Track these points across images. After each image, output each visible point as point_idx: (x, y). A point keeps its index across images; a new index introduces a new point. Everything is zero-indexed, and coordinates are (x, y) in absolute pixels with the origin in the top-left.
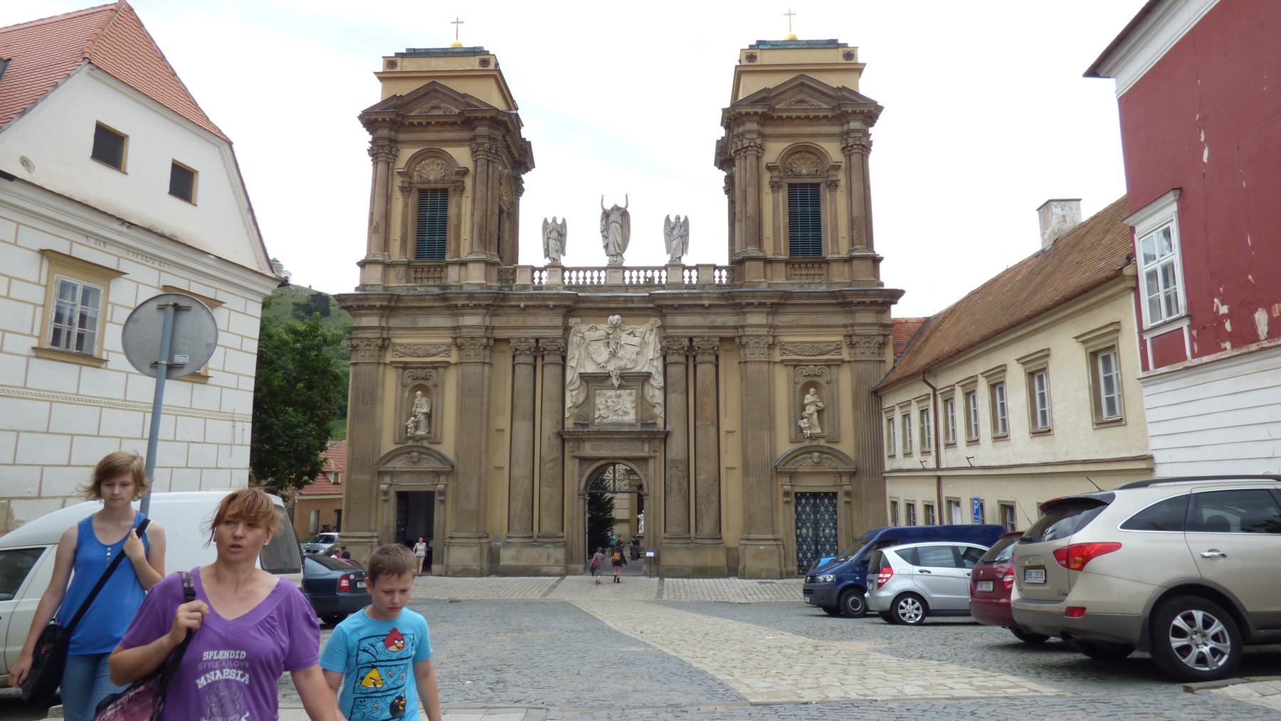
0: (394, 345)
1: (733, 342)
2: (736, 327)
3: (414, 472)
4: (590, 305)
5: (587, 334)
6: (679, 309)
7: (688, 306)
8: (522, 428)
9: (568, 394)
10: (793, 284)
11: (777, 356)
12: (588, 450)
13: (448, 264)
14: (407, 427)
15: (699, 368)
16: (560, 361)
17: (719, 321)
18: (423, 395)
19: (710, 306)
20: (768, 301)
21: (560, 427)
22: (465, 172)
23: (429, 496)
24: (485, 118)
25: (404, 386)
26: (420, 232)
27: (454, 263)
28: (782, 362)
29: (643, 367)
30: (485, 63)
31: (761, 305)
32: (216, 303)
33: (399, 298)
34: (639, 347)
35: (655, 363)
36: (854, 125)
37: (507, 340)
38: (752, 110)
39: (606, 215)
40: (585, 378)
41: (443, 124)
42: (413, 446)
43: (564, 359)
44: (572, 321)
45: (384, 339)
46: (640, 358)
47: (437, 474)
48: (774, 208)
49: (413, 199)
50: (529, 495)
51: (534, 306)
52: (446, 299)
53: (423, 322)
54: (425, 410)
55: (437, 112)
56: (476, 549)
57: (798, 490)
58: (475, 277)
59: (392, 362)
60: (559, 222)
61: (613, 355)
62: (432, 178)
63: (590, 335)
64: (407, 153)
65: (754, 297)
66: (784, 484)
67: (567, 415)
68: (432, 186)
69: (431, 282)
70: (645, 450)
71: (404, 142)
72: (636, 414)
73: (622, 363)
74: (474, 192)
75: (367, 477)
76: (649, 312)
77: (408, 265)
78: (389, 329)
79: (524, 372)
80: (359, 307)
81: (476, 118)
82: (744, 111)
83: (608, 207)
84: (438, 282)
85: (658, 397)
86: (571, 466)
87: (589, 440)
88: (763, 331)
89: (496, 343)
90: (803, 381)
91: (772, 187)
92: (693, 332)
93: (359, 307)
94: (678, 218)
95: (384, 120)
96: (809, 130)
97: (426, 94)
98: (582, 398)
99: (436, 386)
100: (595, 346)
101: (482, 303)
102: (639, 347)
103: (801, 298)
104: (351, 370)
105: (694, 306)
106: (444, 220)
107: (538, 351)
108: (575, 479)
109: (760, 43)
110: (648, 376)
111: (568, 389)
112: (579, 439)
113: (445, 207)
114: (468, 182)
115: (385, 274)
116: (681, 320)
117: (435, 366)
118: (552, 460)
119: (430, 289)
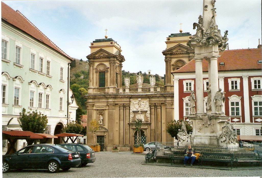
2: (164, 101)
3: (100, 132)
5: (134, 102)
8: (122, 123)
9: (130, 115)
13: (105, 88)
16: (129, 108)
17: (161, 100)
19: (159, 96)
21: (129, 122)
22: (108, 68)
23: (103, 136)
24: (112, 57)
25: (98, 114)
27: (106, 88)
29: (145, 110)
30: (112, 43)
33: (96, 96)
35: (148, 108)
36: (191, 55)
38: (168, 53)
40: (134, 112)
43: (130, 108)
44: (131, 100)
46: (145, 107)
47: (105, 132)
49: (98, 74)
50: (123, 136)
51: (123, 97)
52: (105, 96)
53: (101, 100)
54: (102, 119)
55: (102, 55)
58: (111, 91)
59: (95, 109)
61: (140, 107)
62: (102, 69)
63: (135, 103)
64: (96, 64)
65: (168, 95)
67: (130, 120)
70: (146, 127)
71: (95, 62)
72: (145, 120)
73: (141, 109)
76: (147, 98)
78: (94, 102)
79: (122, 110)
81: (110, 57)
84: (104, 92)
86: (131, 130)
88: (170, 102)
92: (156, 102)
96: (181, 56)
98: (133, 116)
99: (104, 114)
101: (113, 97)
102: (145, 105)
104: (87, 110)
105: (156, 96)
106: (105, 78)
107: (124, 106)
109: (172, 34)
110: (146, 111)
111: (131, 114)
113: (105, 76)
114: (109, 70)
116: (153, 99)
117: (103, 110)
118: (127, 129)
119: (102, 94)
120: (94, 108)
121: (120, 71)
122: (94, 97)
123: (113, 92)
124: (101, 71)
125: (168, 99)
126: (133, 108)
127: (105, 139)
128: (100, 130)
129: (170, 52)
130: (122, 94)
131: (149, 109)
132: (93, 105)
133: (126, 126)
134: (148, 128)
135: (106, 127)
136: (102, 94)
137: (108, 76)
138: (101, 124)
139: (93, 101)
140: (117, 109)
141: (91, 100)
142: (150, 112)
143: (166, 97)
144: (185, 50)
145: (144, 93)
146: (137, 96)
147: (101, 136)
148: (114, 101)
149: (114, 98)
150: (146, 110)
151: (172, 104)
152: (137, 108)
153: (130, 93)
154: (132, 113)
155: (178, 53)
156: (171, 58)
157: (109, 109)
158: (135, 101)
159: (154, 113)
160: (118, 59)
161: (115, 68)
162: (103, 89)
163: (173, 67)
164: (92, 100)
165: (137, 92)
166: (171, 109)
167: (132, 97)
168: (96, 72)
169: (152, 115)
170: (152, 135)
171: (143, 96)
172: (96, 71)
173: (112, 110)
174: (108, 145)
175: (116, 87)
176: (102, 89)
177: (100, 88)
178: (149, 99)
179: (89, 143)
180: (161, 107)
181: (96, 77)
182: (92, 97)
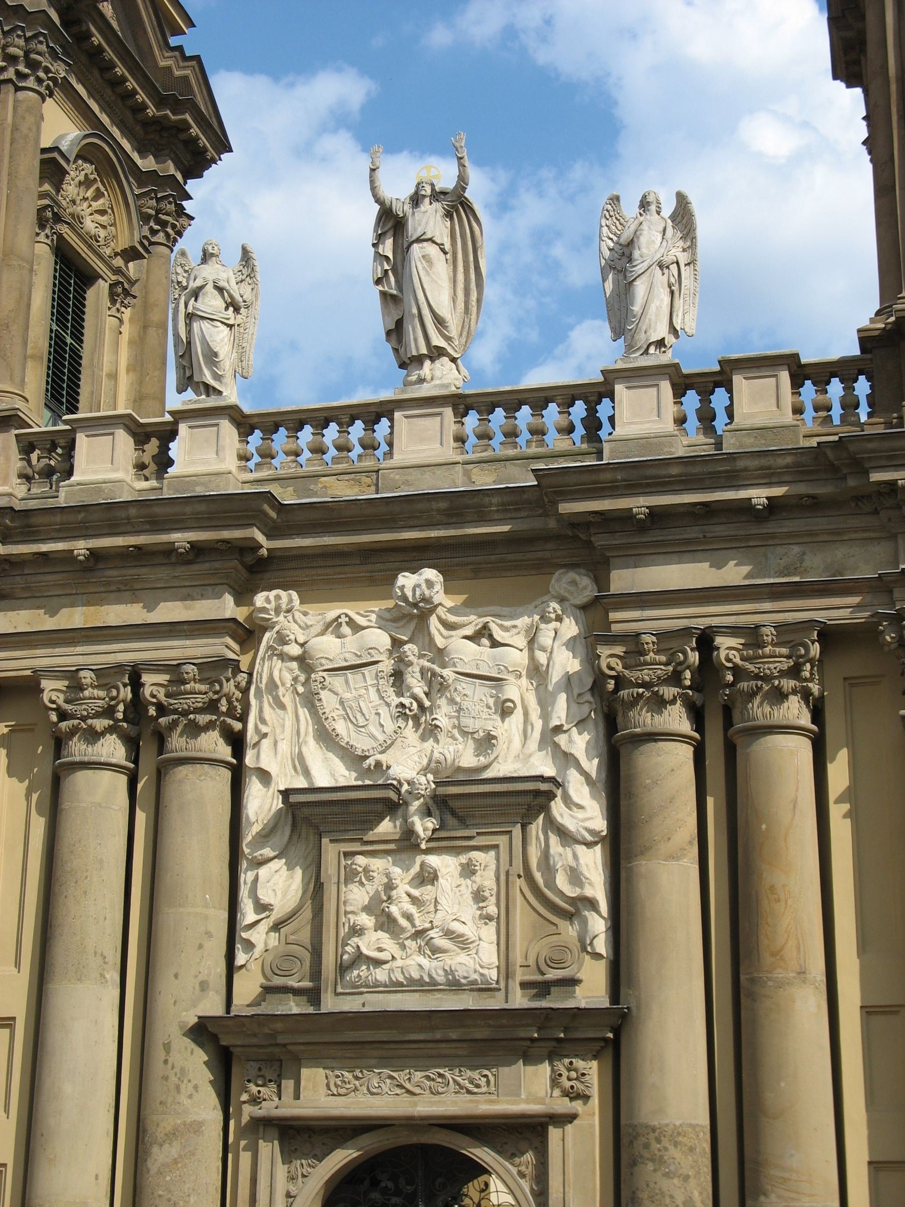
6: (661, 533)
9: (246, 877)
12: (318, 1092)
34: (509, 685)
43: (237, 742)
67: (241, 958)
70: (528, 1088)
126: (290, 755)
134: (571, 1118)
152: (361, 744)
167: (274, 557)
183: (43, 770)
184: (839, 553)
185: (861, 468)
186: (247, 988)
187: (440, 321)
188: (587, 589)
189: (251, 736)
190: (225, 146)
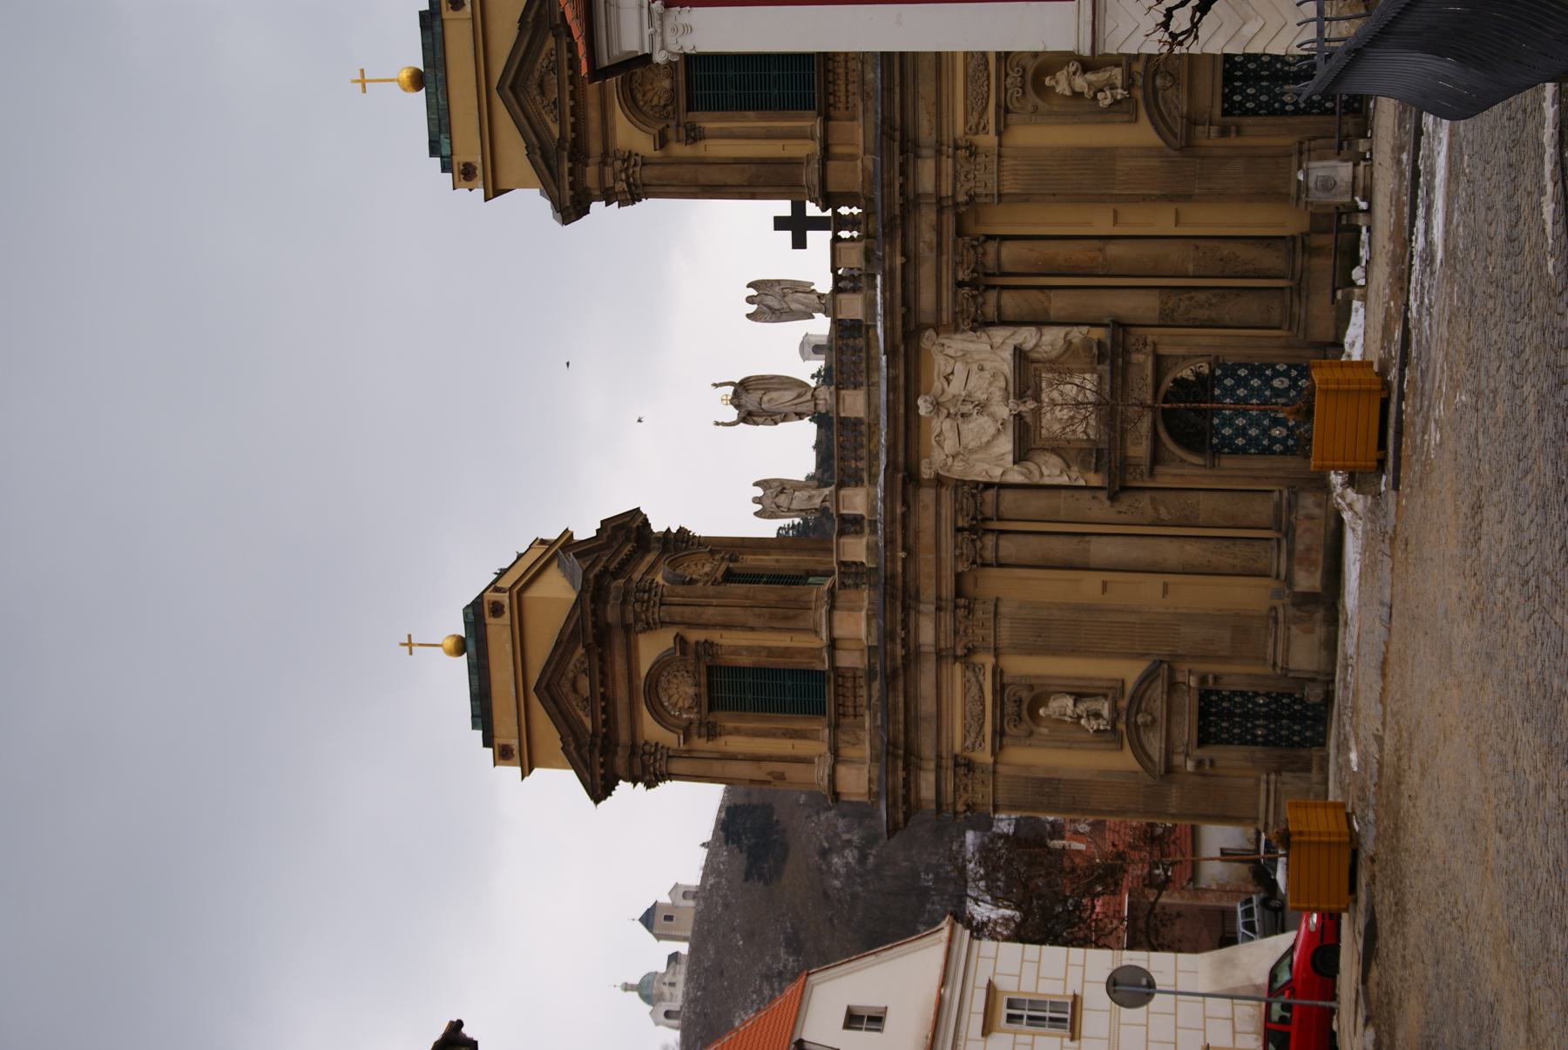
0: (965, 749)
1: (962, 214)
3: (1168, 721)
4: (901, 446)
7: (903, 289)
8: (1102, 550)
9: (1047, 481)
10: (865, 111)
11: (988, 140)
12: (1139, 450)
14: (1098, 731)
15: (1007, 268)
17: (928, 236)
18: (1046, 705)
19: (904, 254)
20: (898, 159)
21: (1103, 495)
22: (681, 640)
23: (1204, 695)
24: (594, 613)
25: (1031, 734)
26: (781, 709)
27: (832, 659)
28: (999, 133)
29: (1004, 362)
30: (497, 609)
31: (903, 173)
32: (991, 989)
33: (892, 744)
37: (959, 577)
38: (567, 179)
39: (747, 417)
40: (1022, 453)
41: (604, 677)
42: (1128, 722)
43: (988, 486)
44: (926, 473)
45: (956, 765)
46: (988, 365)
47: (1172, 686)
48: (731, 138)
49: (726, 720)
50: (1211, 544)
51: (904, 537)
52: (895, 671)
53: (927, 706)
54: (1069, 701)
55: (584, 683)
56: (1294, 630)
57: (1217, 111)
58: (855, 624)
59: (994, 753)
60: (759, 492)
61: (982, 407)
62: (691, 691)
63: (950, 445)
64: (651, 729)
65: (891, 184)
66: (1208, 138)
67: (1082, 483)
68: (704, 690)
69: (863, 692)
70: (1143, 361)
73: (998, 395)
74: (715, 626)
75: (1174, 792)
77: (835, 727)
78: (939, 757)
79: (1009, 548)
80: (906, 800)
81: (595, 625)
82: (568, 193)
83: (732, 414)
84: (862, 682)
85: (1052, 339)
87: (1123, 447)
88: (947, 165)
89: (962, 596)
90: (1032, 98)
91: (695, 140)
92: (947, 280)
93: (906, 800)
94: (750, 300)
95: (603, 765)
97: (555, 701)
98: (1054, 460)
99: (1031, 687)
100: (970, 440)
101: (899, 617)
103: (892, 101)
105: (904, 280)
106: (759, 672)
108: (1185, 469)
109: (434, 150)
110: (1020, 354)
111: (1036, 479)
112: (1125, 464)
113: (739, 671)
114: (695, 636)
115: (849, 761)
116: (927, 299)
117: (1000, 689)
118: (1156, 510)
119: (875, 694)
120: (984, 756)
121: (712, 553)
122: (899, 753)
123: (863, 613)
124: (705, 700)
125: (927, 183)
126: (994, 459)
127: (1226, 687)
128: (1154, 721)
129: (560, 160)
130: (881, 544)
131: (999, 334)
132: (962, 771)
133: (1123, 518)
135: (1130, 671)
136: (875, 694)
137: (742, 643)
138: (1105, 712)
139: (932, 765)
140: (995, 583)
141: (923, 785)
142: (1024, 329)
143: (912, 197)
144: (550, 43)
145: (878, 368)
146: (902, 429)
147: (1203, 714)
148: (932, 608)
149: (913, 603)
150: (1007, 354)
151: (961, 153)
152: (992, 431)
153: (873, 479)
154: (1031, 465)
155: (569, 103)
156: (605, 154)
157: (996, 649)
158: (938, 442)
159: (1035, 292)
160: (623, 564)
161: (680, 589)
162: (837, 686)
163: (678, 141)
164: (922, 774)
165: (864, 428)
166: (1007, 162)
167: (907, 468)
168: (712, 733)
169: (1046, 311)
170: (1204, 314)
171: (902, 380)
172: (704, 730)
173: (1005, 624)
174: (1275, 664)
175: (828, 583)
176: (837, 695)
177: (830, 707)
178: (921, 328)
179: (1256, 806)
180: (990, 238)
181: (747, 735)
182: (895, 769)
183: (995, 572)
184: (924, 226)
185: (893, 218)
186: (1095, 480)
187: (799, 396)
188: (930, 333)
189: (986, 479)
190: (638, 509)
